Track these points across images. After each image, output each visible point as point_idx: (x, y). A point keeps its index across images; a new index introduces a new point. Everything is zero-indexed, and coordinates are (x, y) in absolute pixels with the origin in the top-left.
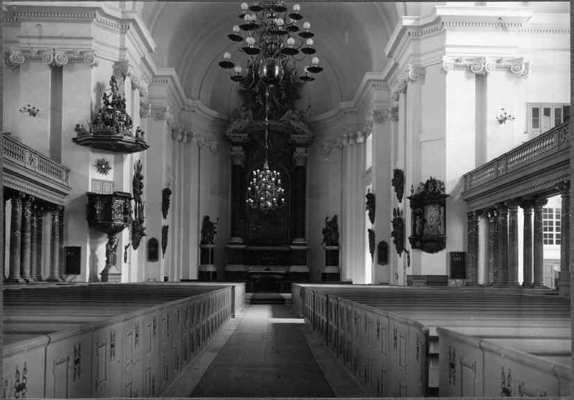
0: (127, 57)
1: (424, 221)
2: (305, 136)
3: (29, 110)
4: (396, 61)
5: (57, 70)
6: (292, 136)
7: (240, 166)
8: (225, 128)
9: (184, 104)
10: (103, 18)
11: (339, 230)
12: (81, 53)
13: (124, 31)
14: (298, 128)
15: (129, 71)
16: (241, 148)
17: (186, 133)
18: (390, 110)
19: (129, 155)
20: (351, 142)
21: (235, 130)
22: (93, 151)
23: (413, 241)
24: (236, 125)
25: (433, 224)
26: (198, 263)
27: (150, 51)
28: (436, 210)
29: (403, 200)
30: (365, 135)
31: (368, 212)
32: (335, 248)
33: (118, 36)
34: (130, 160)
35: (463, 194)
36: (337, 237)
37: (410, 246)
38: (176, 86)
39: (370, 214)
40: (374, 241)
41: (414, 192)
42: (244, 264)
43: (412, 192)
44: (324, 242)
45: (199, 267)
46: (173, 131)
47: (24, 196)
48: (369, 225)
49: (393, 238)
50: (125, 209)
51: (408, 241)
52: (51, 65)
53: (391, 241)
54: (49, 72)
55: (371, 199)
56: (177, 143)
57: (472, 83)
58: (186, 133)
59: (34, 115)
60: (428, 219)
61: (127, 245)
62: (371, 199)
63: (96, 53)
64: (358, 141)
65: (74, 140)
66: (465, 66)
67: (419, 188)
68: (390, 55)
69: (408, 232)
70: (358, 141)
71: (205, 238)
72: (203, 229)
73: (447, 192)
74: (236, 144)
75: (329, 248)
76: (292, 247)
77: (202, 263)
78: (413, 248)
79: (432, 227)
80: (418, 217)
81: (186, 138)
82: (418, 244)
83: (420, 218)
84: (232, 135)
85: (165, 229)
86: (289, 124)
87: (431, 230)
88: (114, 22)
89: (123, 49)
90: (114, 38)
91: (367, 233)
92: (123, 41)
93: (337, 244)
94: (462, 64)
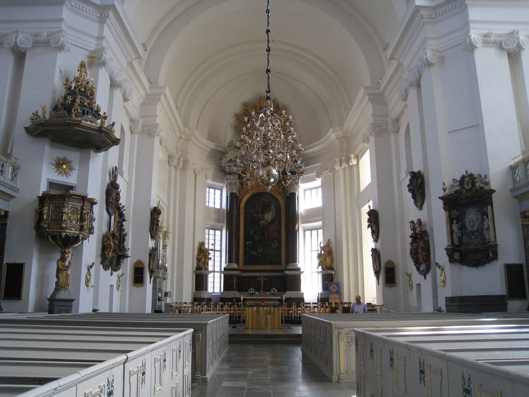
4: (400, 61)
7: (236, 194)
8: (221, 159)
12: (48, 35)
13: (102, 20)
15: (103, 58)
17: (182, 159)
18: (390, 122)
19: (101, 155)
20: (344, 165)
21: (231, 160)
22: (51, 146)
25: (475, 229)
27: (139, 57)
28: (476, 212)
30: (358, 158)
33: (96, 26)
35: (512, 191)
36: (332, 261)
39: (373, 232)
40: (380, 261)
41: (447, 191)
42: (239, 291)
43: (444, 190)
45: (194, 294)
46: (169, 157)
50: (82, 213)
56: (173, 168)
57: (504, 62)
58: (182, 159)
61: (91, 264)
63: (63, 33)
64: (351, 164)
66: (495, 43)
67: (452, 186)
68: (392, 58)
70: (351, 164)
72: (199, 255)
73: (493, 186)
75: (325, 272)
76: (286, 272)
77: (196, 290)
78: (451, 261)
79: (473, 233)
80: (455, 221)
81: (181, 163)
83: (457, 223)
84: (229, 164)
88: (91, 9)
89: (101, 38)
92: (101, 30)
93: (332, 269)
94: (492, 39)
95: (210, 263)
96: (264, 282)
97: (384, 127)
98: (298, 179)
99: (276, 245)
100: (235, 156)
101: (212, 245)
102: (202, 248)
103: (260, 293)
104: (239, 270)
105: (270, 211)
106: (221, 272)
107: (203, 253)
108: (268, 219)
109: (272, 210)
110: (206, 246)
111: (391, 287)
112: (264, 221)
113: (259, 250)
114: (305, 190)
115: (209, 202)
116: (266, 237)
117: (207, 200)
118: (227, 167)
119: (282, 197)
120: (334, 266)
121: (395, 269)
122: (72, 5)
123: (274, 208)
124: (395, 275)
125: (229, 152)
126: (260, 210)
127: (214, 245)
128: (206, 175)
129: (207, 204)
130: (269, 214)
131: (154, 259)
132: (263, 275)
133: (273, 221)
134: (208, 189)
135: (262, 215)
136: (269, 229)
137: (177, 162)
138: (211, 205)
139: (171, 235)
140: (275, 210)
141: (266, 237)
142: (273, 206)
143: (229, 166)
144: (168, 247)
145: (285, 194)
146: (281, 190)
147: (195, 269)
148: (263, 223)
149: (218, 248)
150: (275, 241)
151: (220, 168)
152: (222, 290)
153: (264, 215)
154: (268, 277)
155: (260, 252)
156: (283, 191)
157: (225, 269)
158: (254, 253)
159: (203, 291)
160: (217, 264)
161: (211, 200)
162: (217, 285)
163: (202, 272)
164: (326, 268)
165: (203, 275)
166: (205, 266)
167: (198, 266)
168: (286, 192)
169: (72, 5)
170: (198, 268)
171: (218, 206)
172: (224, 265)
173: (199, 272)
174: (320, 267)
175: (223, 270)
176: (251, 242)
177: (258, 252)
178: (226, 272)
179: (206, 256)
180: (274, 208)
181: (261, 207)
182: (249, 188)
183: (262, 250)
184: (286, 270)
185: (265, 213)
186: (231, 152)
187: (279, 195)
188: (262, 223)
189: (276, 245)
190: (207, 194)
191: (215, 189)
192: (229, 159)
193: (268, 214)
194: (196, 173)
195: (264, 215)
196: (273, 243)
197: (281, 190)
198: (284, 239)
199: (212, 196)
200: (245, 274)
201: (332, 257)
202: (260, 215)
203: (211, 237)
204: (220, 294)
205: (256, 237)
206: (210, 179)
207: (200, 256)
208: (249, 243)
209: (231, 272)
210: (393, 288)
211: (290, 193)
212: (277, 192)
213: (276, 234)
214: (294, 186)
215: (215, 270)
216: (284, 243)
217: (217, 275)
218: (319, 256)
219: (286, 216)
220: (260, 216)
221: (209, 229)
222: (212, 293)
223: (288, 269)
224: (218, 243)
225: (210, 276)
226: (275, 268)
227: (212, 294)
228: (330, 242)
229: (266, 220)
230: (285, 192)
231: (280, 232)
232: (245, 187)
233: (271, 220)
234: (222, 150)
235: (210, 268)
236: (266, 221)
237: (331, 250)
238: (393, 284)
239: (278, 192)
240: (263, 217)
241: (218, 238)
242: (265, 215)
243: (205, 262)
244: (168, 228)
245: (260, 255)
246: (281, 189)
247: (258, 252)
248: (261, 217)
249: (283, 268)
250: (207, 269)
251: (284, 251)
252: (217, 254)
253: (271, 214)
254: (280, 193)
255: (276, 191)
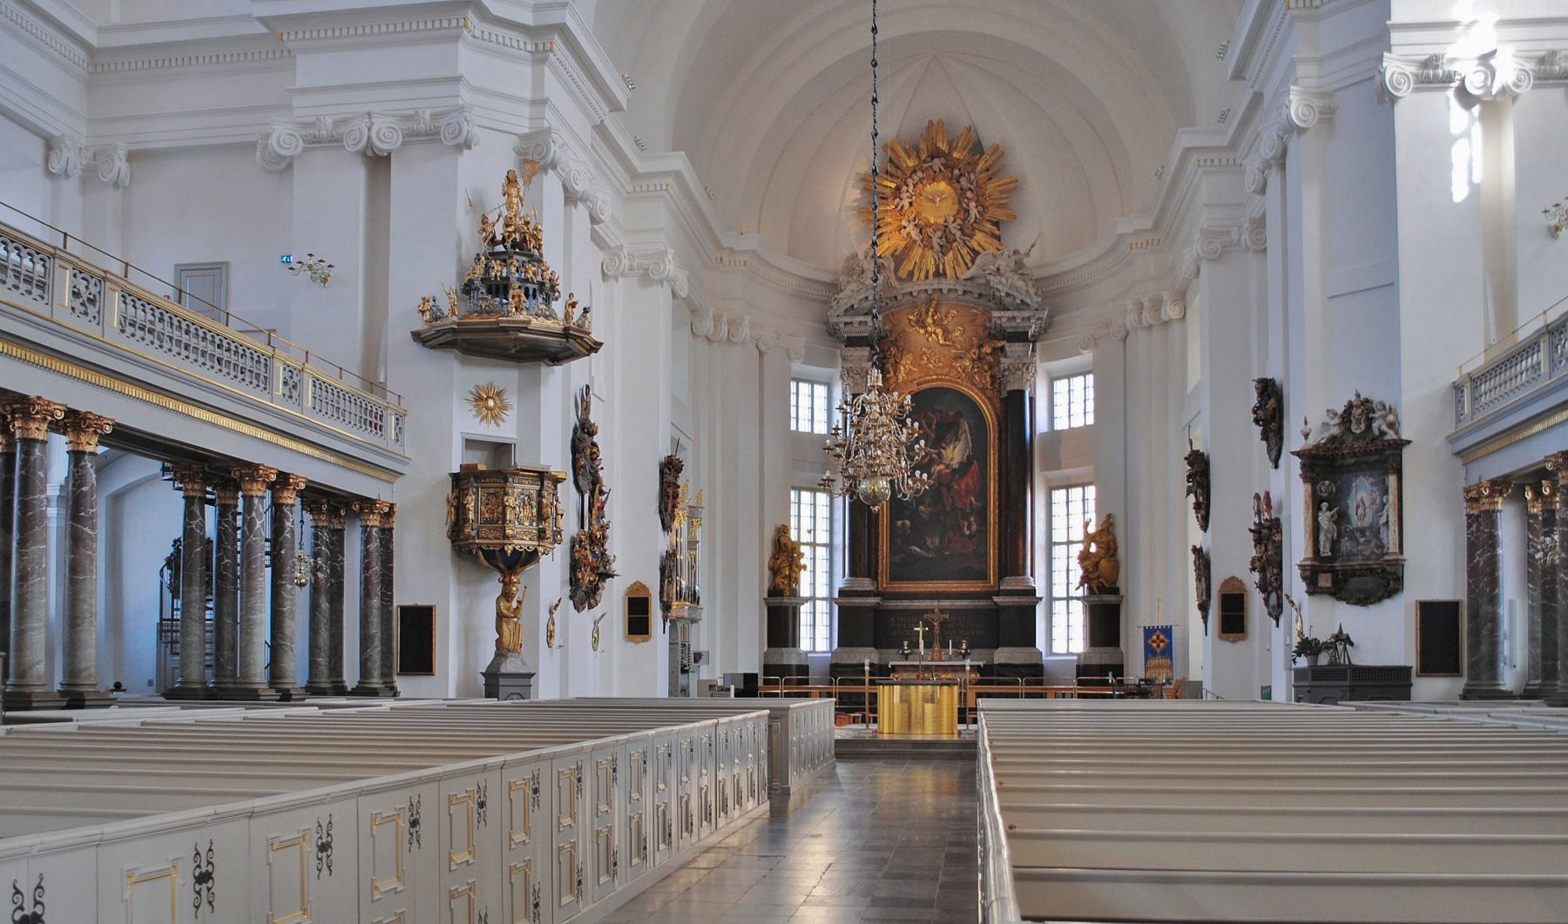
0: (550, 120)
1: (1341, 518)
2: (1026, 314)
3: (310, 267)
5: (378, 163)
6: (996, 314)
8: (826, 303)
9: (719, 247)
10: (487, 28)
11: (1121, 552)
14: (1007, 294)
16: (866, 351)
21: (852, 306)
23: (1311, 576)
24: (851, 294)
26: (761, 644)
29: (1282, 462)
31: (1192, 499)
32: (1110, 599)
34: (560, 382)
36: (1116, 568)
37: (1303, 586)
38: (690, 198)
42: (876, 648)
44: (1082, 584)
47: (273, 478)
48: (1196, 537)
49: (1256, 576)
51: (1297, 573)
52: (364, 154)
53: (1252, 579)
54: (358, 175)
55: (1199, 470)
59: (325, 280)
60: (1352, 512)
62: (1199, 470)
65: (417, 336)
69: (1297, 548)
71: (779, 580)
74: (853, 342)
75: (1095, 599)
76: (996, 599)
81: (725, 328)
82: (1325, 581)
85: (668, 567)
86: (988, 282)
87: (1362, 540)
90: (516, 76)
91: (1192, 557)
95: (805, 577)
96: (941, 624)
97: (1235, 236)
98: (1033, 356)
99: (974, 527)
100: (863, 296)
101: (809, 532)
102: (782, 539)
103: (933, 653)
104: (876, 594)
105: (957, 439)
106: (830, 599)
107: (785, 554)
108: (952, 460)
109: (963, 437)
110: (793, 536)
111: (1233, 642)
112: (942, 467)
113: (929, 541)
114: (1052, 380)
115: (797, 418)
116: (948, 509)
117: (793, 414)
118: (842, 326)
119: (989, 399)
120: (1121, 584)
121: (1245, 597)
122: (474, 37)
123: (967, 429)
124: (1245, 613)
125: (846, 287)
126: (933, 436)
127: (813, 531)
128: (788, 350)
129: (793, 427)
130: (954, 448)
131: (671, 576)
132: (938, 606)
133: (965, 466)
134: (793, 385)
135: (937, 450)
136: (956, 487)
137: (712, 327)
138: (804, 427)
139: (705, 514)
140: (971, 435)
141: (948, 509)
142: (967, 426)
143: (846, 324)
144: (699, 546)
145: (999, 392)
146: (987, 383)
147: (766, 596)
148: (940, 471)
149: (822, 537)
150: (972, 519)
151: (825, 327)
152: (836, 646)
153: (943, 451)
154: (952, 611)
155: (931, 547)
156: (992, 384)
157: (842, 593)
158: (918, 549)
159: (787, 649)
160: (822, 579)
161: (804, 413)
162: (822, 632)
163: (785, 601)
164: (1098, 588)
165: (786, 609)
166: (790, 586)
167: (774, 587)
168: (1000, 387)
169: (474, 37)
170: (774, 592)
171: (821, 428)
172: (840, 583)
173: (776, 601)
174: (1086, 585)
175: (836, 595)
176: (908, 522)
177: (927, 549)
178: (845, 601)
179: (792, 561)
180: (968, 432)
181: (933, 427)
182: (900, 377)
183: (937, 542)
184: (998, 593)
185: (944, 445)
186: (853, 286)
187: (981, 395)
188: (937, 470)
189: (974, 527)
190: (793, 398)
191: (812, 382)
192: (849, 305)
193: (952, 446)
194: (763, 348)
195: (943, 451)
196: (966, 523)
197: (987, 383)
198: (994, 511)
199: (804, 402)
200: (893, 604)
201: (1116, 561)
202: (932, 450)
203: (806, 511)
204: (830, 655)
205: (921, 507)
206: (798, 359)
207: (779, 561)
208: (903, 524)
209: (857, 601)
210: (1241, 645)
211: (1009, 392)
212: (979, 389)
213: (973, 499)
214: (1020, 373)
215: (817, 596)
216: (994, 524)
217: (822, 607)
218: (1084, 557)
219: (1000, 451)
220: (931, 453)
221: (799, 489)
222: (810, 652)
223: (1003, 590)
224: (822, 525)
225: (805, 609)
226: (972, 589)
227: (809, 655)
228: (1111, 520)
229: (947, 462)
230: (997, 386)
231: (983, 494)
232: (889, 378)
233: (961, 463)
234: (827, 278)
235: (805, 591)
236: (947, 466)
237: (1115, 543)
238: (1240, 635)
239: (981, 386)
240: (939, 455)
241: (823, 512)
242: (945, 449)
243: (790, 576)
244: (699, 498)
245: (930, 556)
246: (988, 379)
247: (923, 546)
248: (934, 455)
249: (990, 587)
250: (794, 593)
251: (994, 545)
252: (822, 553)
253: (960, 446)
254: (983, 390)
255: (974, 385)
